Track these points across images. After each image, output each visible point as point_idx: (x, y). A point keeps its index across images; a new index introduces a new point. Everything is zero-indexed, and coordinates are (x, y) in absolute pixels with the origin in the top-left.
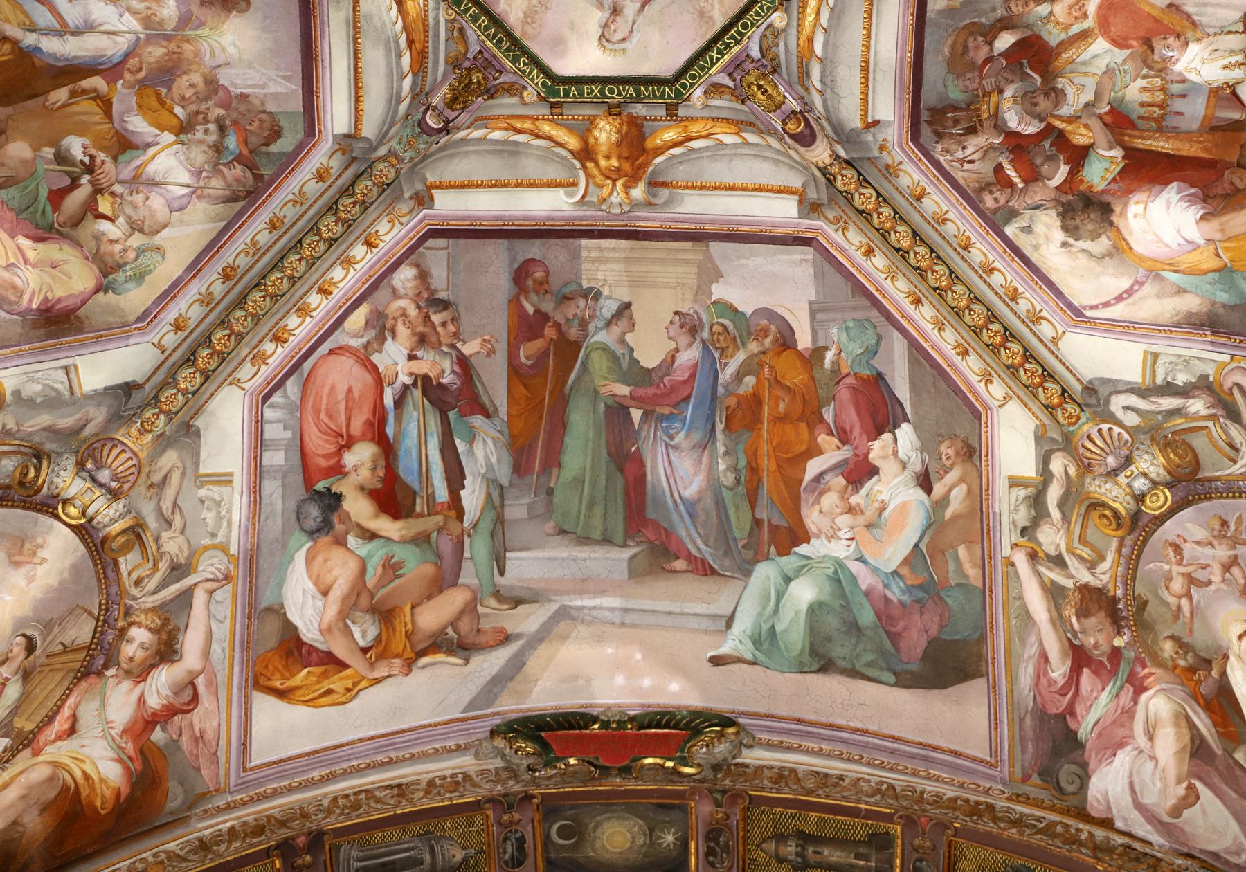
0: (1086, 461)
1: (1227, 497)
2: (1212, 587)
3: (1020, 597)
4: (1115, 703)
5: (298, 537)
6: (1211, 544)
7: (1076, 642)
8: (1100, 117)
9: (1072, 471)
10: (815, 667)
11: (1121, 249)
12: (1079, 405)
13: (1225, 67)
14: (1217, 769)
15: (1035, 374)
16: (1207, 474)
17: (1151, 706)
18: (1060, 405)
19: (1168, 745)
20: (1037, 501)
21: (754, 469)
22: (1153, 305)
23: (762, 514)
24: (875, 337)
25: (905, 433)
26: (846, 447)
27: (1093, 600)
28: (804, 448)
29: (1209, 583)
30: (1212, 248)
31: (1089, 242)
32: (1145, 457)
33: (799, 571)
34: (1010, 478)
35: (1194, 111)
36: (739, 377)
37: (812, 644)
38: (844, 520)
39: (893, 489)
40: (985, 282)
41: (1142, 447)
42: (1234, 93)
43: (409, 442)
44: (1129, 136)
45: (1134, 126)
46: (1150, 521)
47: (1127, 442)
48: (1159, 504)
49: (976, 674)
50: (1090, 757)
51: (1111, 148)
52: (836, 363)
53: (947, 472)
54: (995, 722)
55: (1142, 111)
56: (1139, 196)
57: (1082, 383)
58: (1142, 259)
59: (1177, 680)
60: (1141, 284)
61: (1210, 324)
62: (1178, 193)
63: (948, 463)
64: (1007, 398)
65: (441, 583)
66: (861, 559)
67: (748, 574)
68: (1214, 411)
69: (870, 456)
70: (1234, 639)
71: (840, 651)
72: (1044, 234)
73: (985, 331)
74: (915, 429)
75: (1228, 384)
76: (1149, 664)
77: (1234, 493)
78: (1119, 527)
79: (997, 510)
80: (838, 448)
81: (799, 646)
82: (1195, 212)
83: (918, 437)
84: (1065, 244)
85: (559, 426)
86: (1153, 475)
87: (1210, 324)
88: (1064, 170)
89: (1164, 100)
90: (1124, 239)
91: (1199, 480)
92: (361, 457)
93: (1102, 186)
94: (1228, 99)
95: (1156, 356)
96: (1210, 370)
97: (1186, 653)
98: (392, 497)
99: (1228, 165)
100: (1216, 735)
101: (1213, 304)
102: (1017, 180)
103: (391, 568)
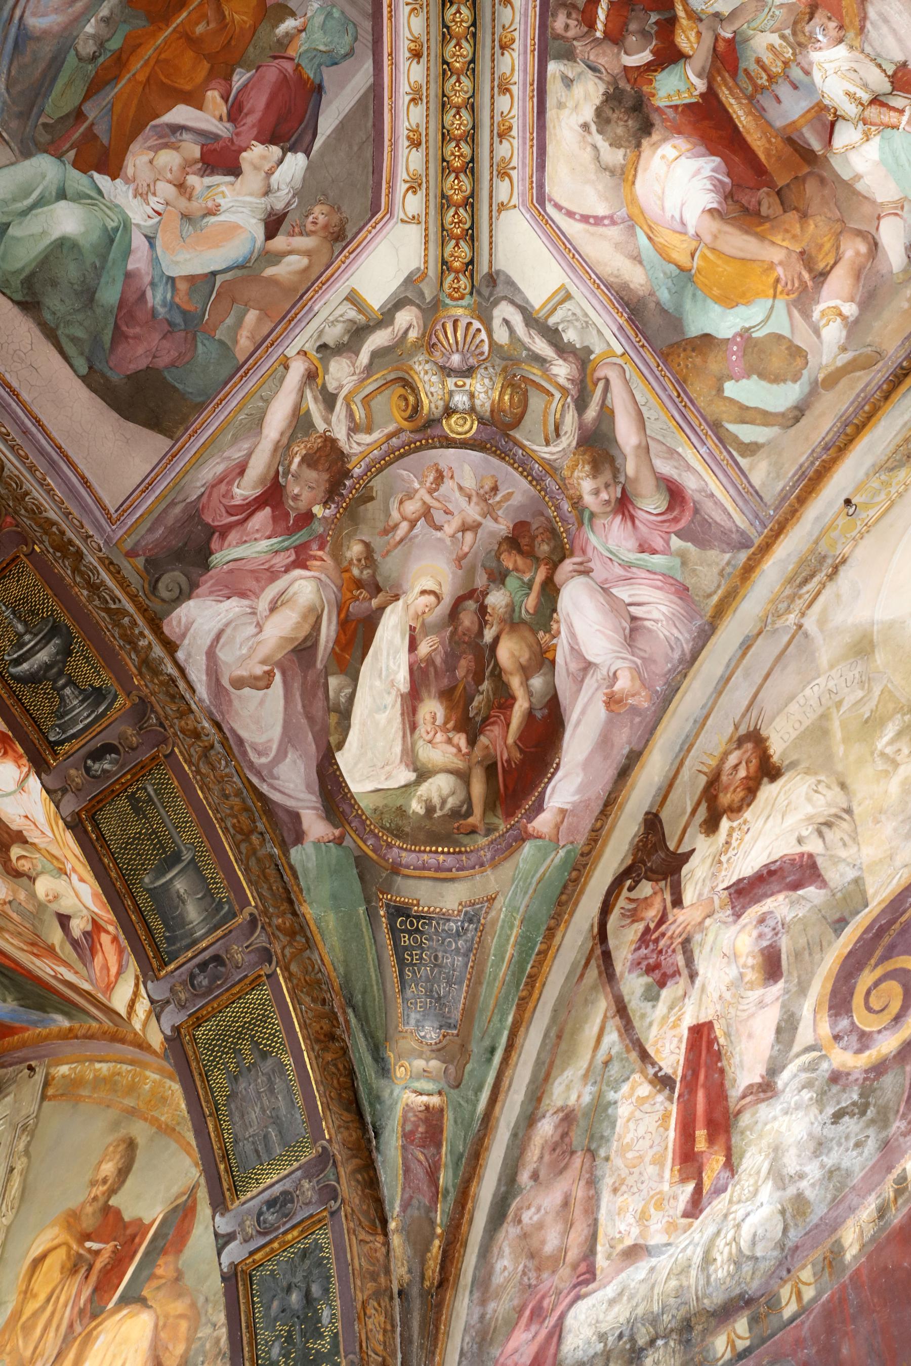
0: (434, 340)
1: (516, 469)
2: (439, 534)
3: (267, 401)
4: (268, 557)
6: (470, 498)
7: (281, 480)
8: (717, 38)
9: (413, 335)
10: (18, 297)
11: (624, 176)
12: (473, 286)
13: (848, 94)
14: (305, 677)
15: (461, 223)
16: (518, 436)
17: (296, 586)
18: (457, 272)
19: (282, 627)
20: (358, 333)
21: (120, 61)
22: (605, 251)
23: (92, 111)
24: (347, 48)
26: (228, 125)
27: (330, 458)
28: (188, 87)
29: (439, 528)
30: (694, 244)
31: (606, 144)
32: (487, 381)
33: (79, 197)
34: (353, 291)
35: (790, 108)
37: (33, 274)
38: (166, 190)
40: (492, 97)
41: (491, 370)
42: (833, 125)
44: (723, 79)
45: (734, 73)
46: (439, 437)
47: (482, 353)
48: (460, 430)
49: (168, 433)
50: (206, 582)
51: (699, 76)
52: (290, 37)
53: (301, 234)
54: (146, 485)
55: (753, 67)
56: (681, 142)
57: (490, 267)
58: (633, 200)
59: (339, 582)
60: (614, 223)
61: (634, 310)
62: (713, 170)
63: (310, 227)
64: (415, 220)
66: (151, 240)
67: (26, 154)
68: (570, 386)
69: (244, 154)
70: (417, 590)
71: (56, 304)
72: (578, 99)
73: (453, 144)
74: (308, 168)
75: (600, 373)
76: (327, 549)
77: (524, 470)
78: (410, 419)
79: (316, 309)
80: (221, 119)
81: (19, 265)
82: (710, 200)
83: (304, 179)
84: (585, 126)
86: (478, 402)
87: (634, 310)
88: (644, 57)
89: (778, 75)
90: (636, 170)
91: (508, 436)
93: (662, 103)
94: (824, 125)
95: (568, 297)
96: (598, 349)
97: (366, 567)
99: (771, 184)
100: (329, 650)
101: (652, 294)
102: (600, 26)
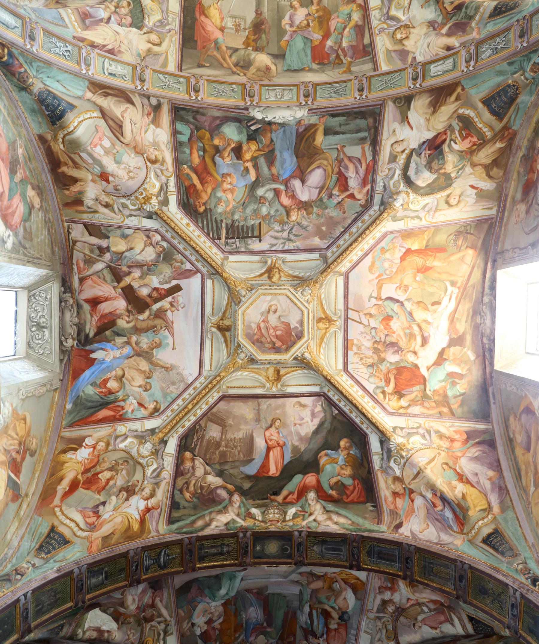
5: (350, 613)
21: (236, 616)
23: (234, 607)
25: (198, 632)
33: (224, 596)
36: (240, 636)
38: (213, 610)
39: (200, 620)
43: (321, 626)
65: (315, 592)
66: (208, 603)
67: (237, 592)
85: (284, 622)
92: (333, 626)
98: (326, 615)
103: (328, 598)
